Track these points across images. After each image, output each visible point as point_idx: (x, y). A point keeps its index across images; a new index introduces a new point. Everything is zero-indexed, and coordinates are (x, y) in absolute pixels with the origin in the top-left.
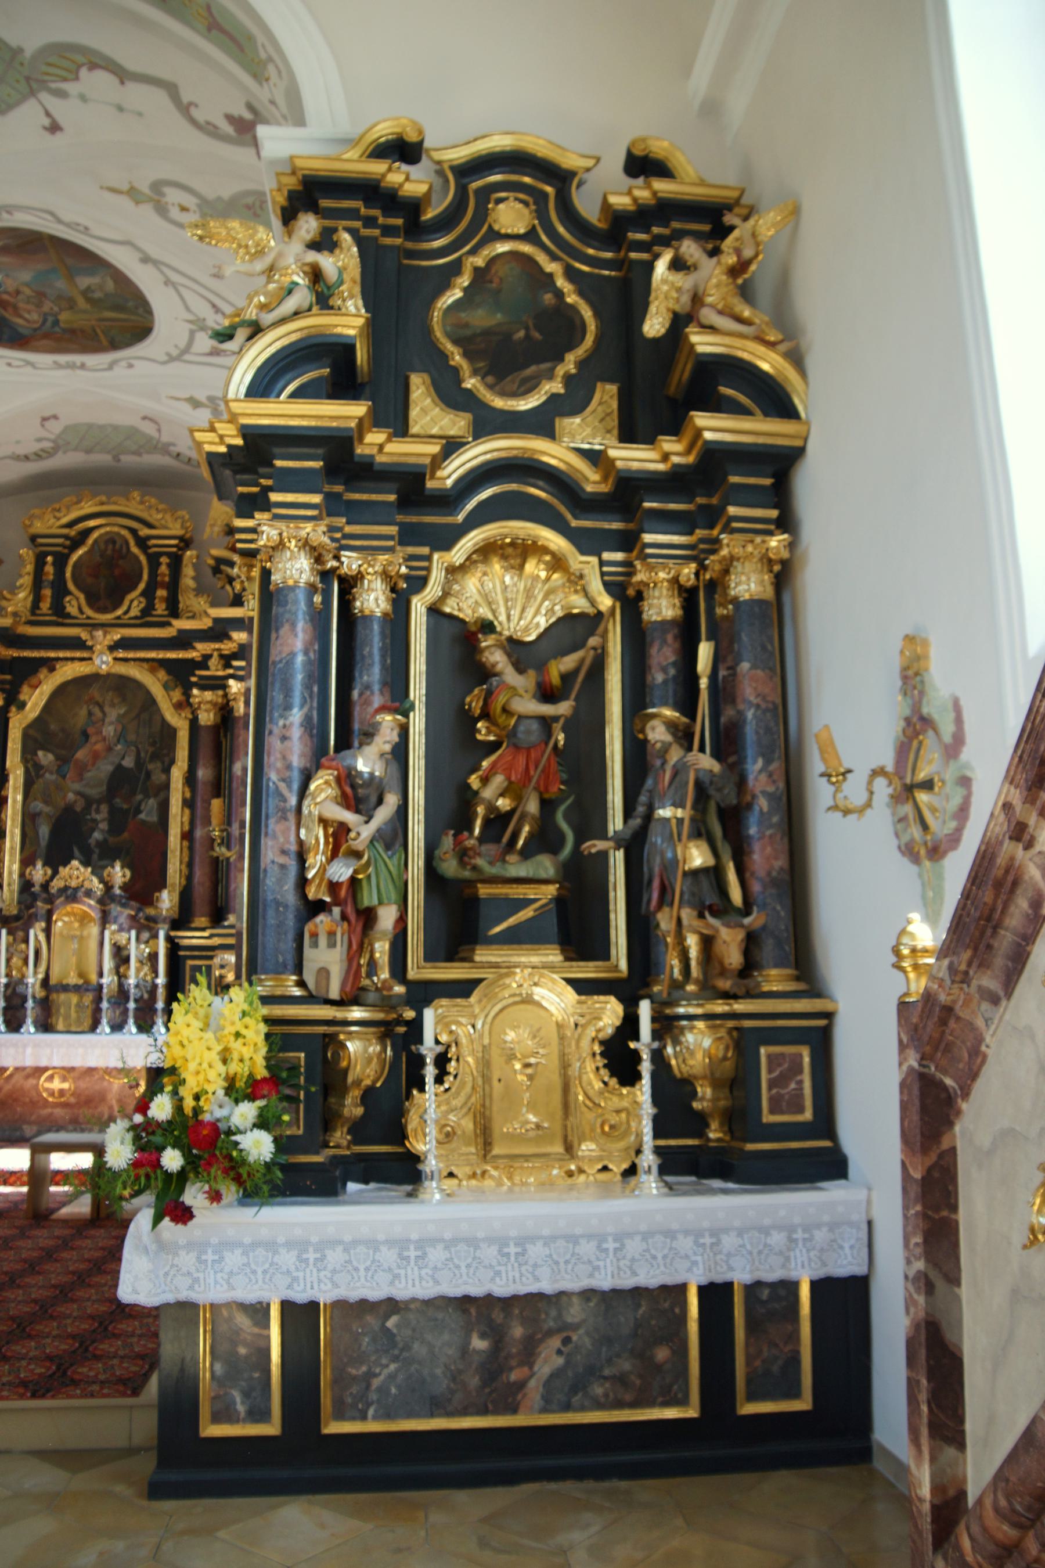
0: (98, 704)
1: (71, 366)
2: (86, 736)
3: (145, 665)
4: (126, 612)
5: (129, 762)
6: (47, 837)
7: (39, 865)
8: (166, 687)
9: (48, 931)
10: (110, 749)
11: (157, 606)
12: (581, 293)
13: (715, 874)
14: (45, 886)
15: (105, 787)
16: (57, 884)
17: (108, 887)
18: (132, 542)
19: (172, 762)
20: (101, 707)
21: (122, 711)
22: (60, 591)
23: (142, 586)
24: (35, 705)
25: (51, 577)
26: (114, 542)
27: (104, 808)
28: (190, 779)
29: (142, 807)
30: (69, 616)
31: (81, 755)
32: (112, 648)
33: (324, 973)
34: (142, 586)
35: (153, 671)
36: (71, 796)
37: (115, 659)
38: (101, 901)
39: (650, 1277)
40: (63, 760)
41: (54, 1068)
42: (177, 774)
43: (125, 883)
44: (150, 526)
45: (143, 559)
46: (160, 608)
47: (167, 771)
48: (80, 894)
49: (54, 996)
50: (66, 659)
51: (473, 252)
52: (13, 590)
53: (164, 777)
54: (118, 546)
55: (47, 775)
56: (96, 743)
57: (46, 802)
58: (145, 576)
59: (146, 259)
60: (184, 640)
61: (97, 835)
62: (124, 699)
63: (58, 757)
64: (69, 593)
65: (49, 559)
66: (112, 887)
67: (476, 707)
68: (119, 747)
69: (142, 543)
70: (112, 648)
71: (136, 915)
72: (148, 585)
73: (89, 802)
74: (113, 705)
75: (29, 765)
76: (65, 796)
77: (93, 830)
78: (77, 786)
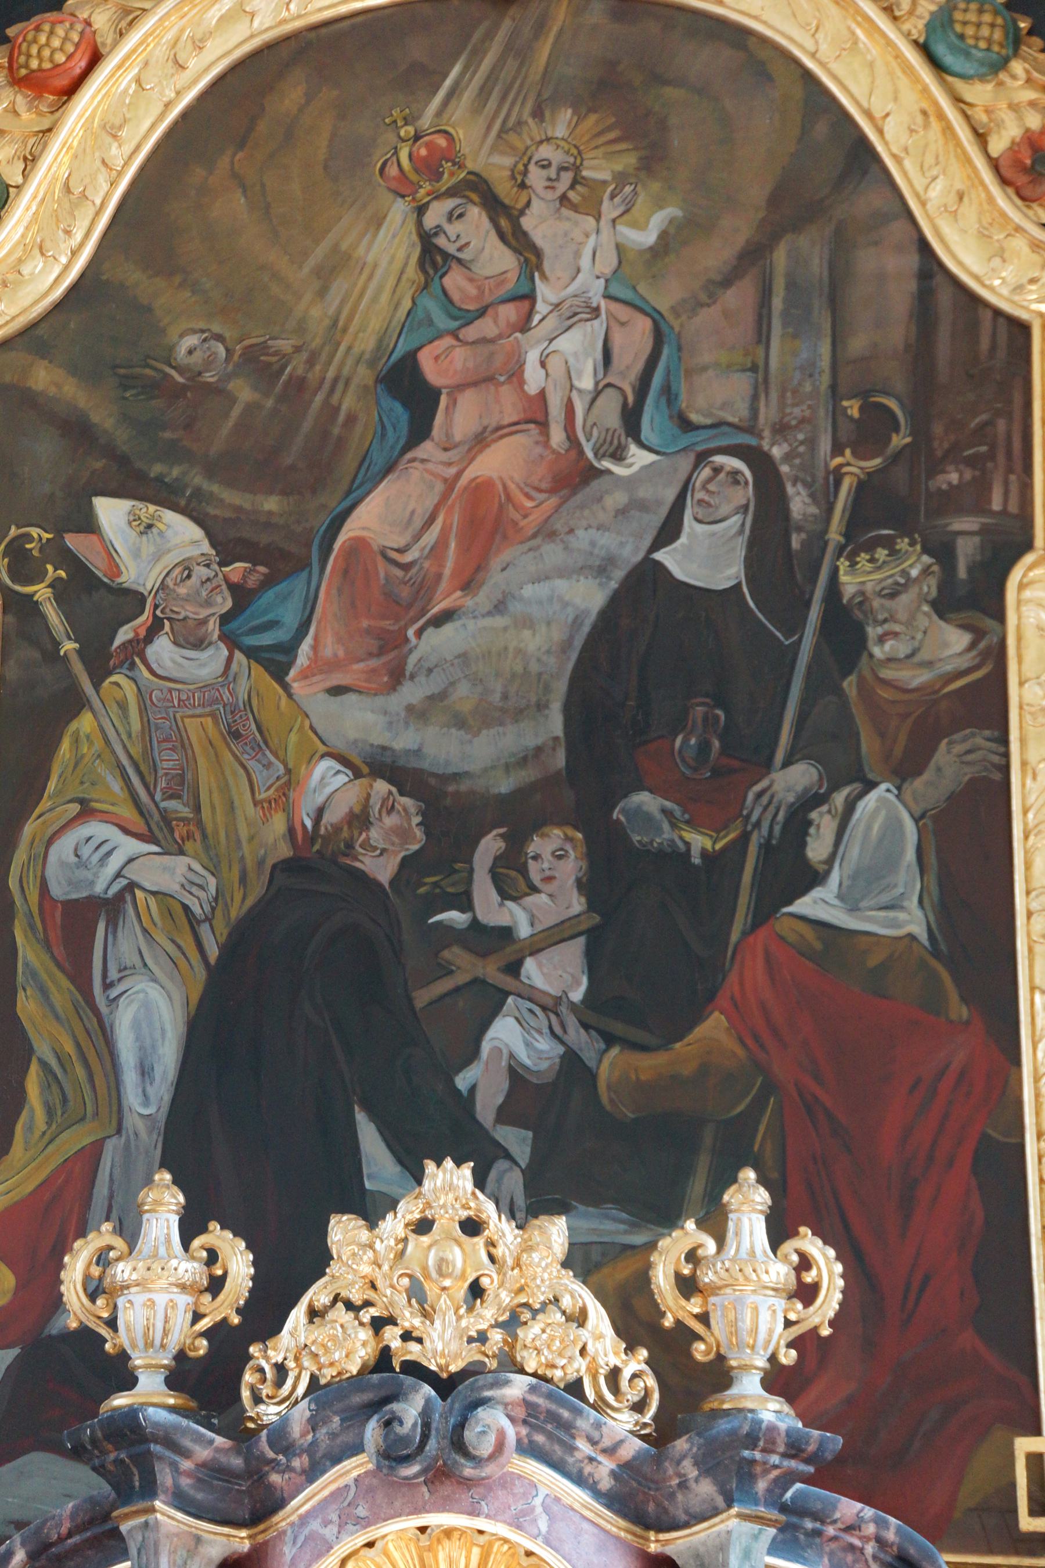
15: (555, 723)
21: (648, 237)
29: (817, 850)
56: (481, 441)
68: (639, 458)
75: (41, 592)
76: (290, 782)
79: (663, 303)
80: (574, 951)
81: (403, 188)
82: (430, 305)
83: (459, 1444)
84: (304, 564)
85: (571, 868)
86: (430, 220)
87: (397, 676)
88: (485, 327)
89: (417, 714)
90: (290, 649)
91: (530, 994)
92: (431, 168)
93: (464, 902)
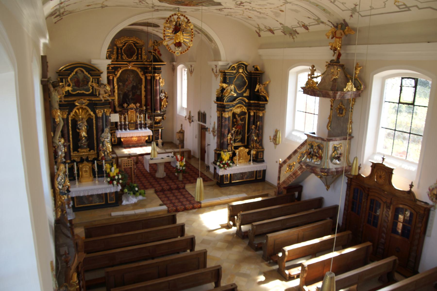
2: (127, 80)
3: (137, 68)
4: (134, 58)
8: (141, 71)
9: (127, 114)
12: (247, 79)
13: (257, 140)
14: (127, 107)
16: (129, 107)
17: (137, 107)
18: (133, 46)
19: (142, 84)
20: (129, 75)
22: (122, 55)
23: (136, 54)
25: (120, 52)
27: (131, 92)
28: (145, 87)
30: (123, 59)
31: (126, 83)
33: (230, 149)
34: (136, 54)
35: (138, 69)
36: (125, 90)
39: (253, 170)
40: (124, 84)
42: (143, 87)
44: (138, 44)
45: (135, 49)
46: (140, 58)
47: (141, 86)
51: (237, 75)
52: (113, 54)
53: (140, 87)
58: (136, 52)
61: (130, 97)
67: (235, 121)
69: (135, 46)
77: (129, 96)
78: (126, 89)
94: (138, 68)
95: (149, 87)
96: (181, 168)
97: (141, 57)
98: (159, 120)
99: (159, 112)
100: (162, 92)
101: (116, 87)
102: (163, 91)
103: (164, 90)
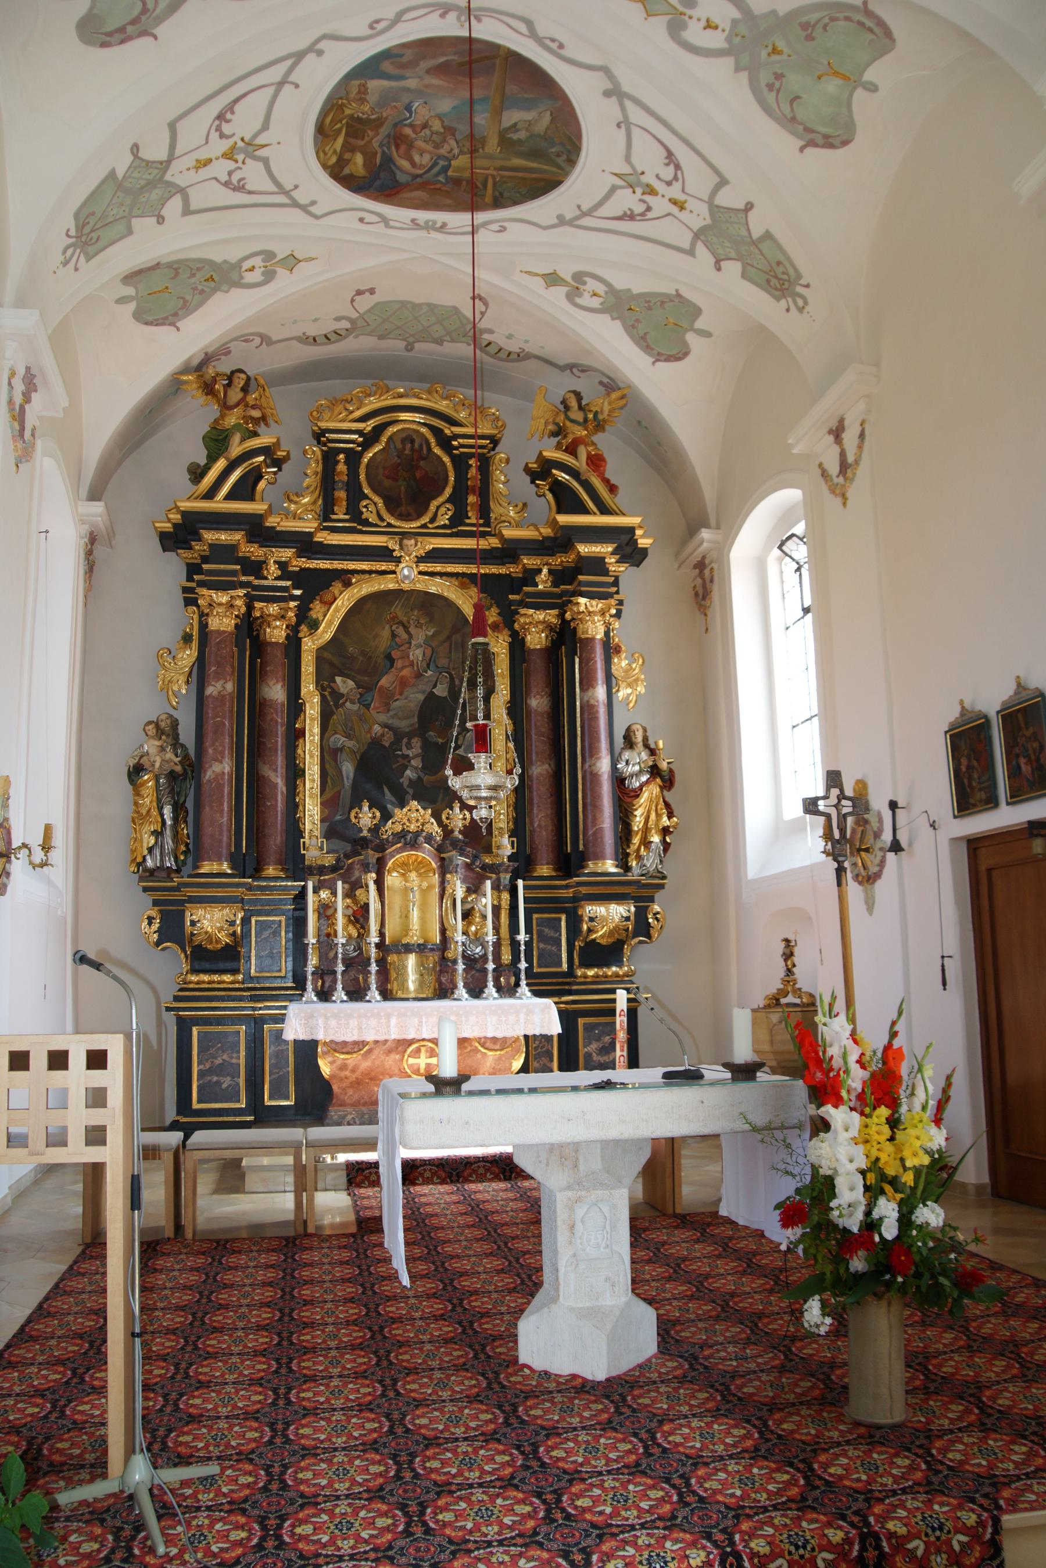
0: (401, 623)
1: (429, 226)
2: (390, 659)
3: (453, 580)
4: (433, 520)
5: (441, 691)
6: (351, 775)
7: (366, 808)
9: (380, 883)
10: (419, 675)
11: (470, 514)
14: (375, 830)
16: (391, 827)
17: (447, 832)
18: (433, 441)
21: (431, 633)
22: (355, 495)
23: (448, 491)
24: (330, 623)
25: (346, 478)
26: (412, 441)
27: (416, 742)
28: (516, 709)
30: (366, 523)
31: (384, 682)
32: (420, 560)
35: (463, 586)
36: (377, 728)
37: (420, 573)
38: (440, 849)
40: (366, 688)
41: (424, 1040)
43: (465, 826)
45: (446, 459)
46: (473, 518)
48: (421, 839)
49: (392, 958)
50: (363, 572)
54: (417, 446)
55: (348, 704)
56: (402, 668)
57: (348, 736)
59: (615, 92)
60: (510, 552)
61: (408, 773)
62: (432, 620)
63: (359, 685)
64: (366, 497)
65: (342, 456)
66: (452, 831)
68: (430, 673)
69: (445, 442)
70: (420, 560)
71: (473, 863)
72: (454, 488)
73: (399, 736)
74: (419, 626)
75: (326, 693)
76: (370, 729)
77: (405, 767)
78: (383, 718)
79: (433, 645)
80: (419, 759)
81: (388, 622)
82: (394, 644)
83: (415, 841)
84: (371, 690)
85: (419, 745)
86: (394, 627)
87: (389, 710)
88: (403, 648)
89: (392, 717)
90: (370, 704)
91: (412, 766)
92: (393, 619)
93: (401, 750)
94: (465, 580)
95: (537, 702)
96: (888, 1210)
97: (484, 511)
98: (611, 933)
99: (610, 866)
100: (629, 741)
101: (312, 709)
102: (639, 737)
103: (645, 730)
